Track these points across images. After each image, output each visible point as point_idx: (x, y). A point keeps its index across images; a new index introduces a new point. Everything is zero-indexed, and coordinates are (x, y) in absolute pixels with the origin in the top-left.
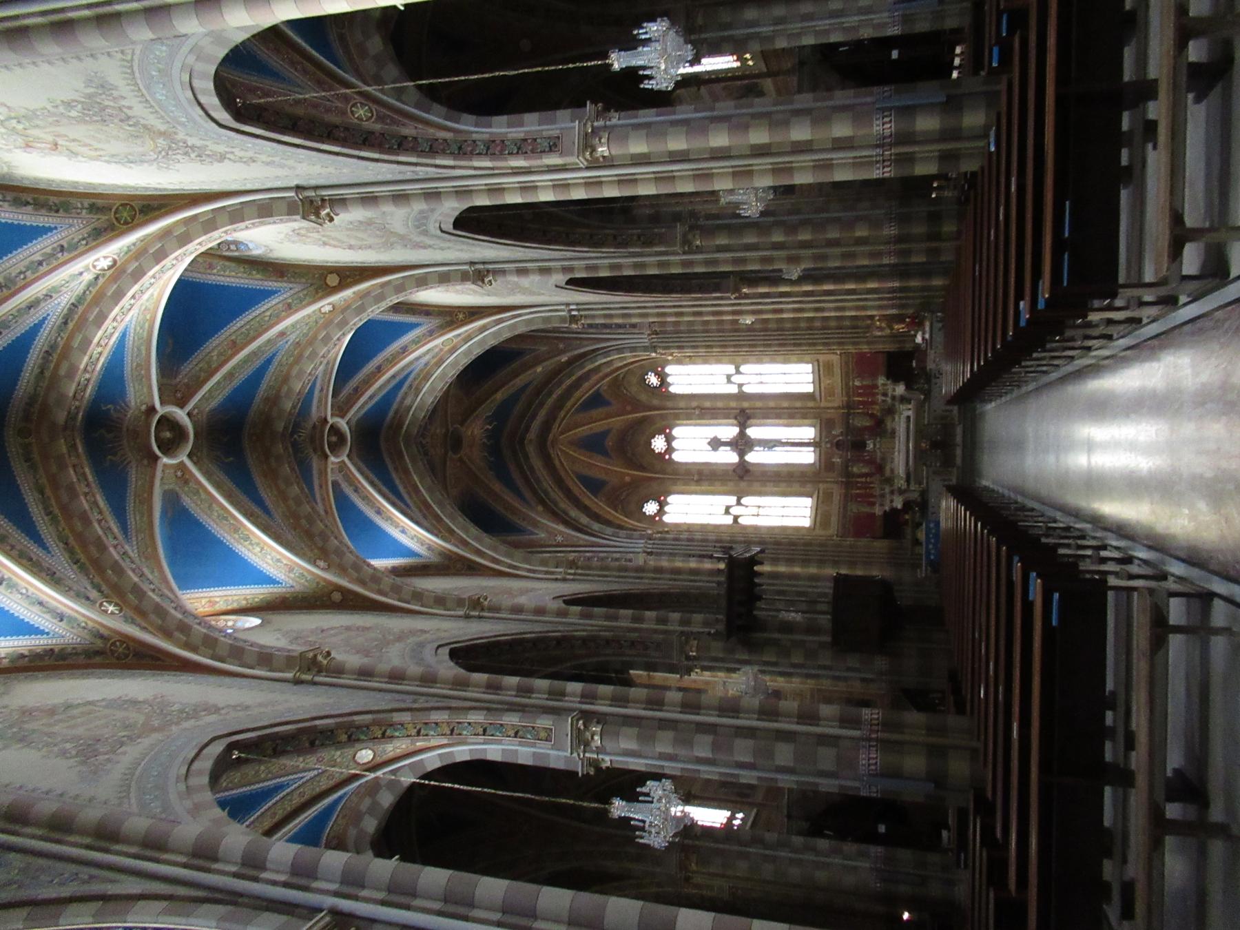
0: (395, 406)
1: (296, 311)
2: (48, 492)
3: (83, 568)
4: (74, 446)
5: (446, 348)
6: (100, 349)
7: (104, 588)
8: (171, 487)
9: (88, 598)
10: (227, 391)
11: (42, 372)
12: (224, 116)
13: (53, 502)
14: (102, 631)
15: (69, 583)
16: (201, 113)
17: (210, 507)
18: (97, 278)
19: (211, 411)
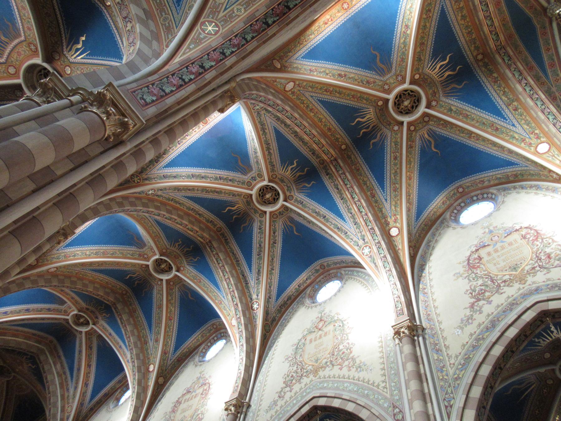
0: (63, 358)
1: (161, 355)
2: (198, 216)
3: (169, 199)
4: (202, 238)
5: (66, 406)
6: (226, 277)
7: (156, 198)
8: (144, 249)
9: (161, 190)
10: (155, 300)
11: (233, 253)
12: (322, 402)
13: (194, 214)
14: (147, 182)
15: (171, 191)
16: (328, 395)
17: (122, 253)
18: (251, 299)
19: (153, 287)
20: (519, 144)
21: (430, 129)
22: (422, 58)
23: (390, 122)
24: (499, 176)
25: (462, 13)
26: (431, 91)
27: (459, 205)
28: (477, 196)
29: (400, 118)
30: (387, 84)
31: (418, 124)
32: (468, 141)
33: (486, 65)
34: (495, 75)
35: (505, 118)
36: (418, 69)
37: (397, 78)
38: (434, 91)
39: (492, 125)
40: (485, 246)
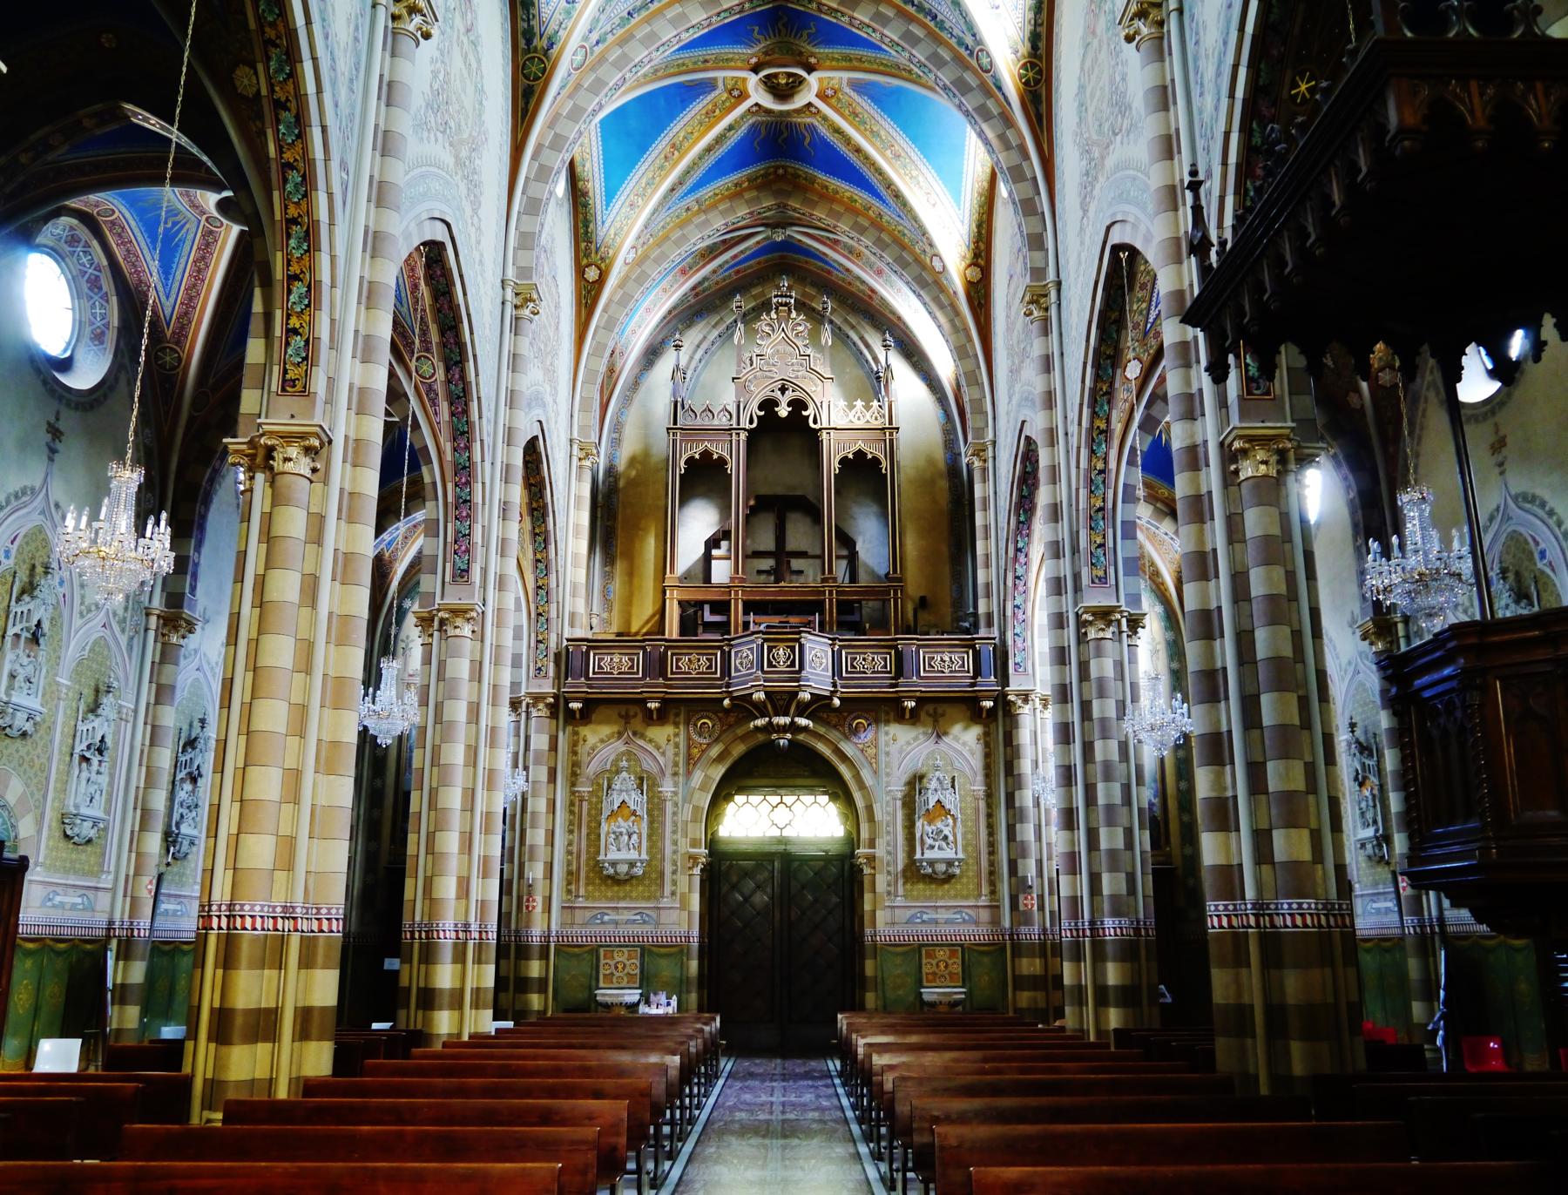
24: (588, 165)
33: (765, 176)
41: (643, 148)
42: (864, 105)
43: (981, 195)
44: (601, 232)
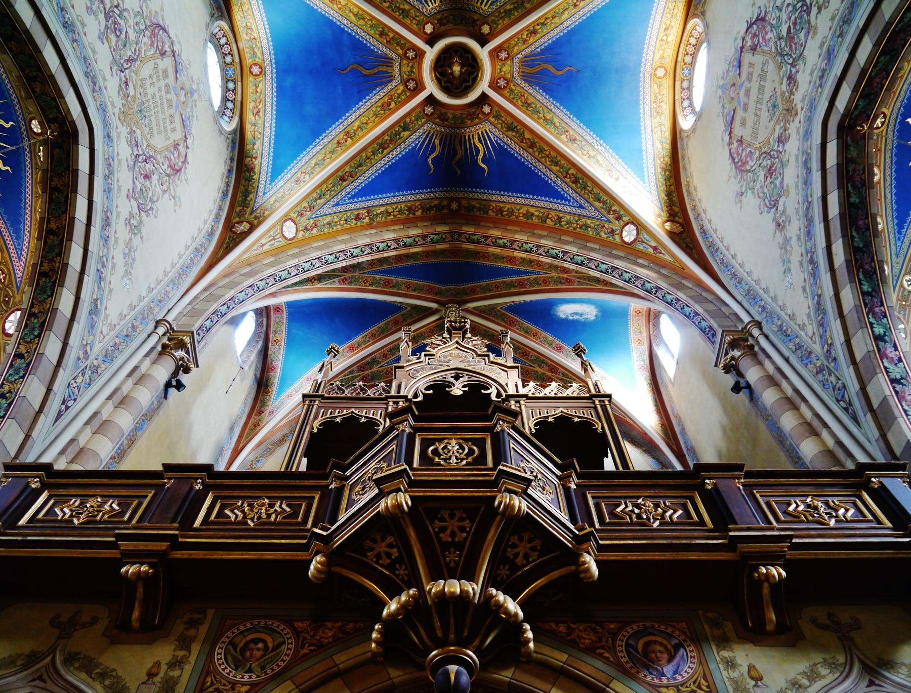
20: (308, 199)
21: (391, 81)
22: (510, 133)
23: (444, 25)
24: (258, 144)
25: (538, 216)
26: (451, 116)
27: (230, 54)
28: (234, 90)
29: (441, 44)
30: (506, 59)
31: (412, 67)
32: (341, 127)
33: (439, 207)
34: (419, 213)
35: (353, 197)
36: (498, 117)
37: (505, 79)
38: (447, 120)
39: (352, 175)
40: (176, 72)
41: (316, 133)
42: (537, 95)
43: (665, 170)
44: (260, 201)
